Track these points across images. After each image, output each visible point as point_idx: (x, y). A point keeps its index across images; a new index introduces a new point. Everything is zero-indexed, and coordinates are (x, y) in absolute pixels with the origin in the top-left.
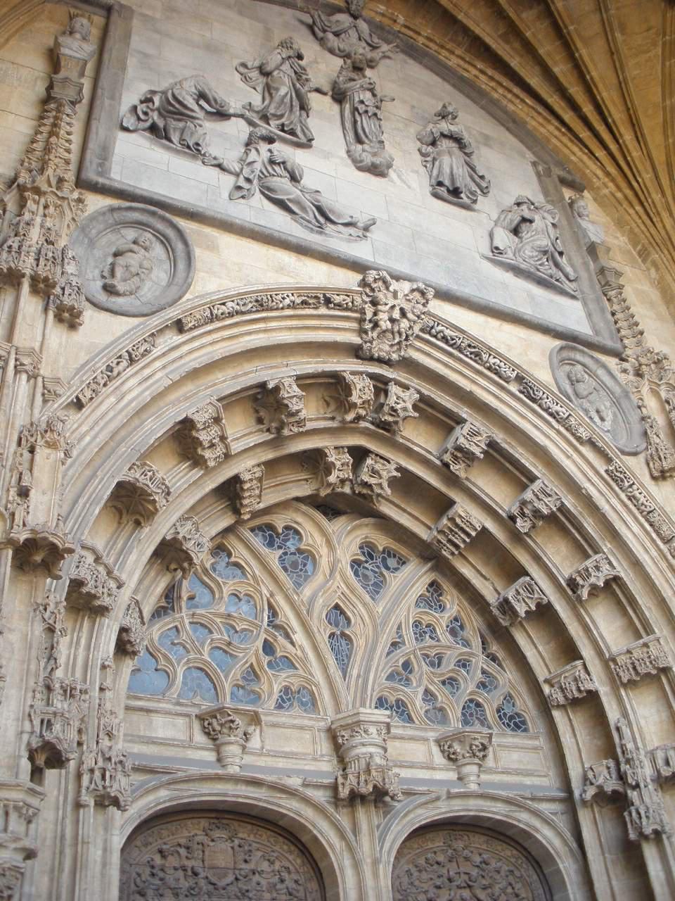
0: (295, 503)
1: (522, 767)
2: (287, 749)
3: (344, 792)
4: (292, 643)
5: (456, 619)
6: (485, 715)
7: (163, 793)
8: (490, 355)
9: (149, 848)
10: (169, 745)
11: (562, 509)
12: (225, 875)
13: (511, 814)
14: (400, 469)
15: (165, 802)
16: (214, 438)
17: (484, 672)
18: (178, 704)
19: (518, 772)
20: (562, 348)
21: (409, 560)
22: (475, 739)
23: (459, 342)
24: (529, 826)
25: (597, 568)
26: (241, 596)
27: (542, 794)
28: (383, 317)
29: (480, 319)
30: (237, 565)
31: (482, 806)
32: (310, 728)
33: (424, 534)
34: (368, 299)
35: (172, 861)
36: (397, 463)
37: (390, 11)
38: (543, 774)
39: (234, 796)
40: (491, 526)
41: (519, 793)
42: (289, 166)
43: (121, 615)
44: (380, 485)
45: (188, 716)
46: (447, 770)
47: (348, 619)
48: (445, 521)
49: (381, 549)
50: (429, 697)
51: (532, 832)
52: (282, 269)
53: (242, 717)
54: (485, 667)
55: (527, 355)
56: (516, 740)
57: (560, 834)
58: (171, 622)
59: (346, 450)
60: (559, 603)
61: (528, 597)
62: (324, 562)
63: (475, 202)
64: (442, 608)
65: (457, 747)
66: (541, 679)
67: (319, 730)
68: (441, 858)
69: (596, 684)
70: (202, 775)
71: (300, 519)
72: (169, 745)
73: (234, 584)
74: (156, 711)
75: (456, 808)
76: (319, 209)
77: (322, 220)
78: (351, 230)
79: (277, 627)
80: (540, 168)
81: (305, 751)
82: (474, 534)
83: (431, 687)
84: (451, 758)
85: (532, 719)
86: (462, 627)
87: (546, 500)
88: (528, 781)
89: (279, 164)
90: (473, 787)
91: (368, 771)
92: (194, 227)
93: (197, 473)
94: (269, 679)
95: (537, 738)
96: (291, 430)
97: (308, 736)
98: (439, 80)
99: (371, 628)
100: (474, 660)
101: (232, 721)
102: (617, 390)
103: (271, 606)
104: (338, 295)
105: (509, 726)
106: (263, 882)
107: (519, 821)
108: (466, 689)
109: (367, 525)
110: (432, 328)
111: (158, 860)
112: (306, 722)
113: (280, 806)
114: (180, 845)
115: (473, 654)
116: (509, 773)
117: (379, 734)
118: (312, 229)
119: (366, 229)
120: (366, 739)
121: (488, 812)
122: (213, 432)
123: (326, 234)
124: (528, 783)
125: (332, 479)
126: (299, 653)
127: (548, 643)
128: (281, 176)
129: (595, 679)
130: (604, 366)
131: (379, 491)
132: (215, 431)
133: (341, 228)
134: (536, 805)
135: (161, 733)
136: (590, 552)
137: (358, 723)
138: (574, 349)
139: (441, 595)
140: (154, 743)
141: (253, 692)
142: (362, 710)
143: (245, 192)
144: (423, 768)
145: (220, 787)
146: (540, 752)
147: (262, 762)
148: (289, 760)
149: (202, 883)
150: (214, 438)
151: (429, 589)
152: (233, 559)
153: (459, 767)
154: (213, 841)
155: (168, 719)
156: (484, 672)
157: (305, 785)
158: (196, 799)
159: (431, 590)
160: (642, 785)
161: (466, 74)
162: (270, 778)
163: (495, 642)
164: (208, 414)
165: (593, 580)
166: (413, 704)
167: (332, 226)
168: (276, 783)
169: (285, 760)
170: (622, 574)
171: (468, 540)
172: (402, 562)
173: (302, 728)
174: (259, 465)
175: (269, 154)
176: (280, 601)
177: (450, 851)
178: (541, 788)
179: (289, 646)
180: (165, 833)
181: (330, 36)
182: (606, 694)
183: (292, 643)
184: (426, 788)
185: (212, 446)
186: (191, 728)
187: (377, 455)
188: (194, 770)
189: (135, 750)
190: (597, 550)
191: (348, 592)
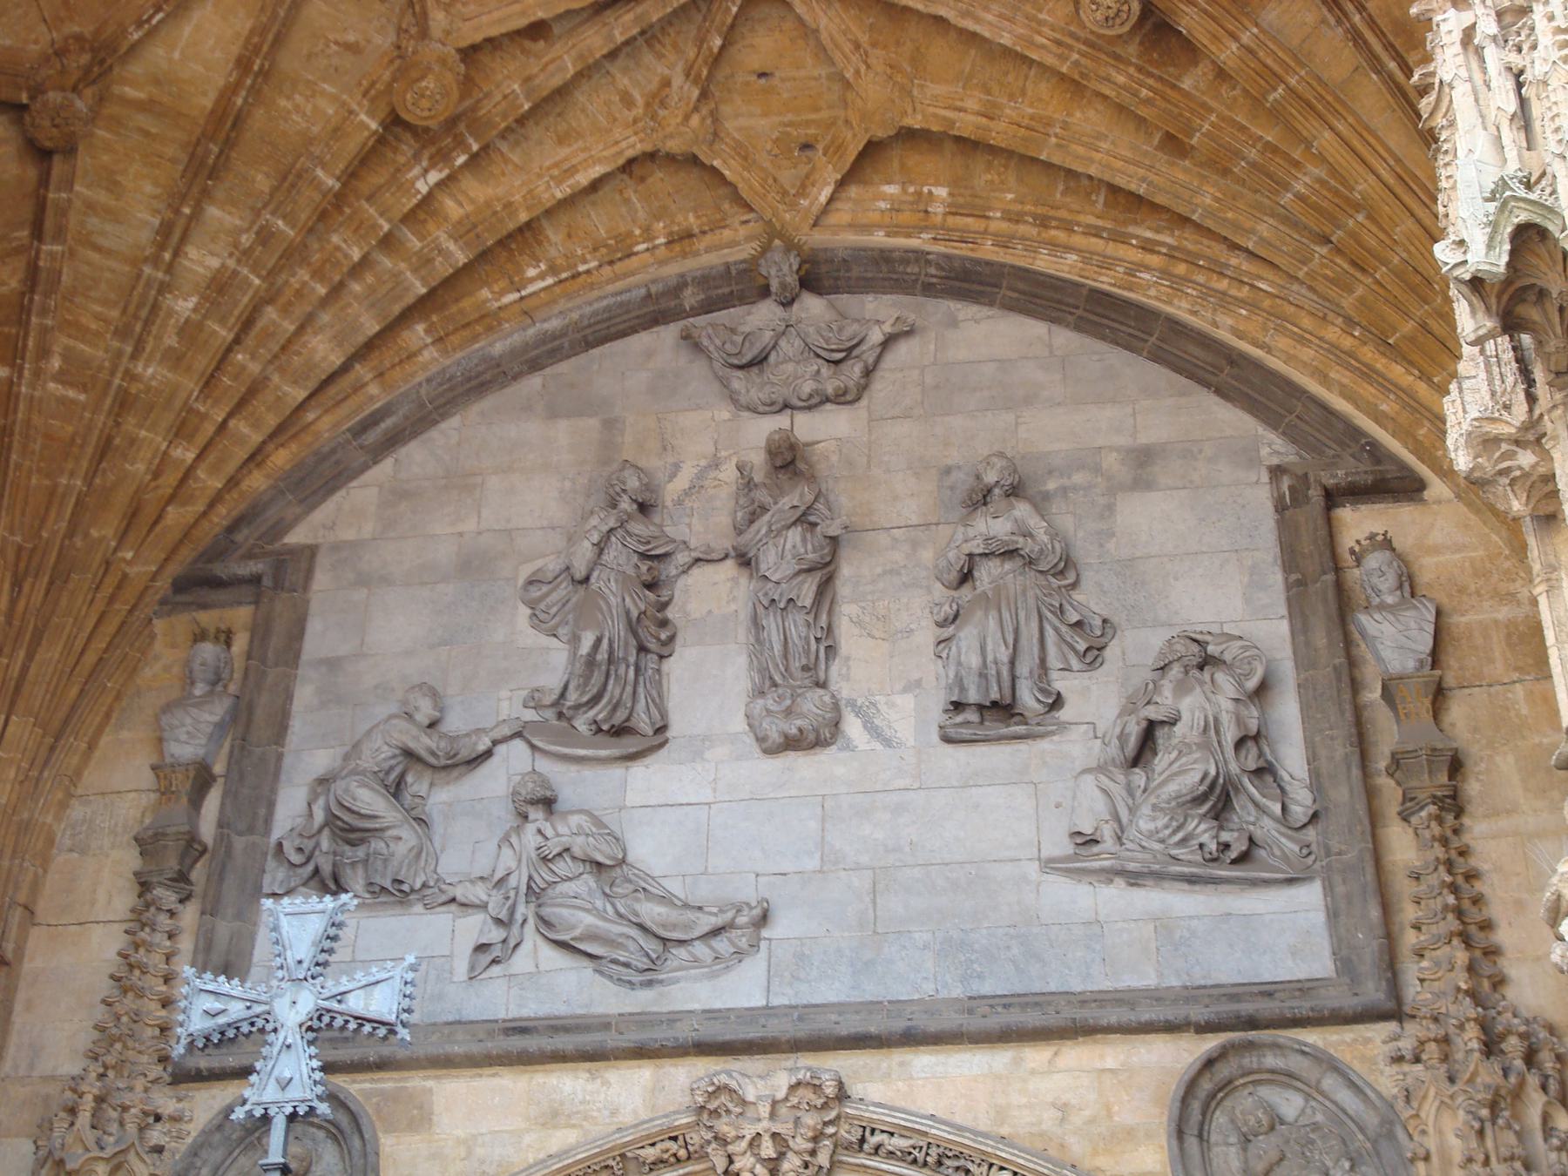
8: (991, 1165)
20: (1209, 1063)
23: (920, 1156)
29: (998, 1059)
34: (709, 1136)
37: (911, 190)
42: (577, 851)
52: (555, 1114)
55: (1110, 1115)
63: (1057, 702)
76: (642, 927)
77: (652, 946)
78: (722, 945)
80: (1286, 483)
89: (560, 854)
92: (389, 1085)
102: (1372, 1120)
104: (653, 1145)
110: (862, 1140)
118: (630, 982)
119: (764, 919)
123: (661, 982)
128: (570, 879)
130: (1334, 1067)
133: (700, 949)
138: (1250, 1046)
143: (496, 952)
161: (1105, 282)
167: (681, 952)
175: (540, 839)
181: (738, 381)
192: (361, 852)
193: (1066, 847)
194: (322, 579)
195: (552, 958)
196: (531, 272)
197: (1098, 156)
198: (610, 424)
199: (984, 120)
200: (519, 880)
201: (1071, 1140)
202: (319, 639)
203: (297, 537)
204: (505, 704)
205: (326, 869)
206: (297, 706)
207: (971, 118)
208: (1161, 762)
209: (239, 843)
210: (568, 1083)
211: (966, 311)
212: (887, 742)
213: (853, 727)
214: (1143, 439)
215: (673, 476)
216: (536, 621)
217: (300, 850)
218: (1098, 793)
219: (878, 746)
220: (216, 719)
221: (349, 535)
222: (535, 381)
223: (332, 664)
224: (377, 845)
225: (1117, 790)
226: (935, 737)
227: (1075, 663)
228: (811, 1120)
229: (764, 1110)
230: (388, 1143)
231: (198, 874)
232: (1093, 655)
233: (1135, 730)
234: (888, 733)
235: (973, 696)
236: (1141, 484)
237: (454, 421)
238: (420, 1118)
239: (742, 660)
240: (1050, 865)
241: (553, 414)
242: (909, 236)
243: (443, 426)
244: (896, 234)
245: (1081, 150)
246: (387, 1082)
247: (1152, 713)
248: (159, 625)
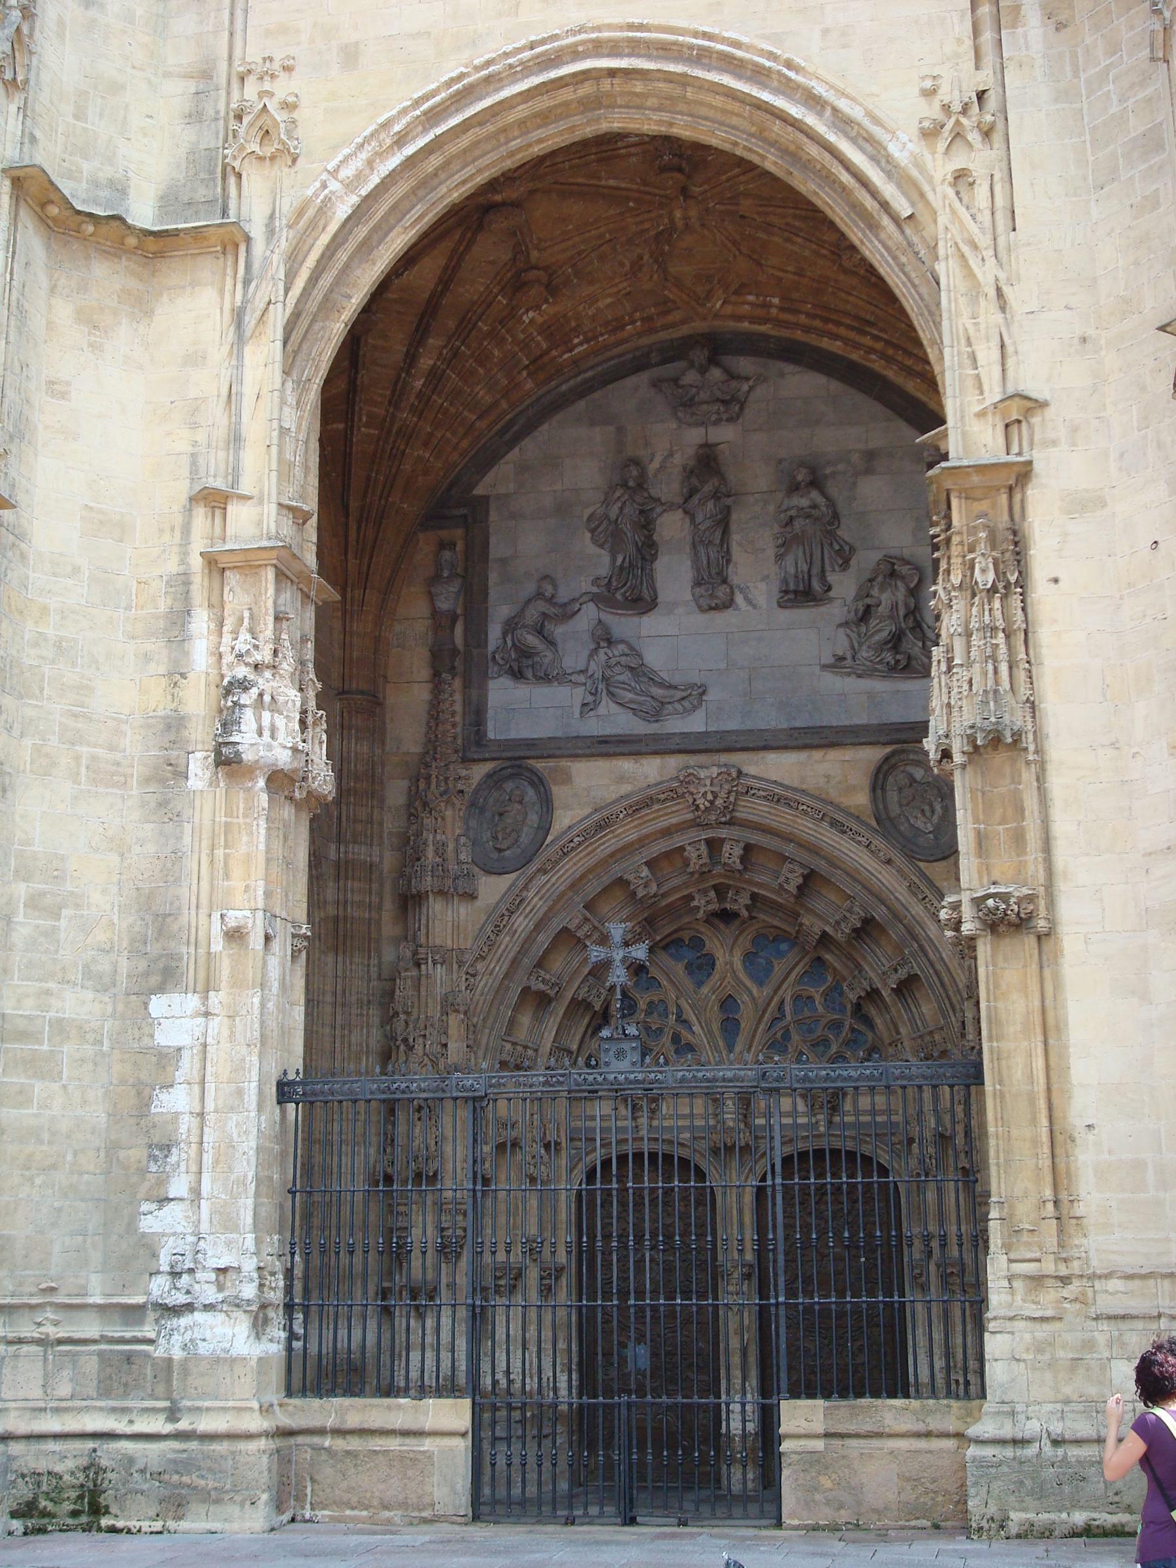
20: (887, 759)
25: (896, 970)
28: (700, 802)
63: (829, 588)
78: (686, 703)
98: (822, 379)
132: (586, 928)
156: (853, 1030)
167: (669, 707)
179: (690, 1037)
192: (530, 662)
193: (831, 660)
194: (493, 516)
195: (614, 708)
196: (576, 341)
197: (851, 299)
198: (620, 430)
199: (796, 278)
200: (598, 675)
201: (831, 791)
202: (497, 548)
203: (479, 491)
204: (583, 584)
205: (516, 668)
206: (491, 583)
207: (791, 276)
208: (873, 622)
209: (475, 652)
210: (626, 765)
211: (789, 368)
212: (755, 607)
213: (739, 599)
214: (872, 445)
215: (652, 460)
216: (594, 541)
217: (503, 659)
218: (846, 639)
219: (749, 608)
220: (455, 590)
221: (502, 490)
222: (581, 404)
223: (503, 561)
224: (537, 659)
225: (854, 636)
226: (775, 605)
227: (837, 568)
228: (727, 787)
229: (708, 782)
230: (555, 790)
231: (458, 663)
232: (845, 565)
233: (861, 609)
234: (754, 602)
235: (792, 587)
236: (869, 471)
237: (545, 426)
238: (567, 779)
239: (689, 563)
240: (825, 667)
241: (593, 423)
242: (760, 324)
243: (540, 429)
244: (754, 323)
245: (843, 295)
246: (551, 763)
247: (868, 601)
248: (421, 536)
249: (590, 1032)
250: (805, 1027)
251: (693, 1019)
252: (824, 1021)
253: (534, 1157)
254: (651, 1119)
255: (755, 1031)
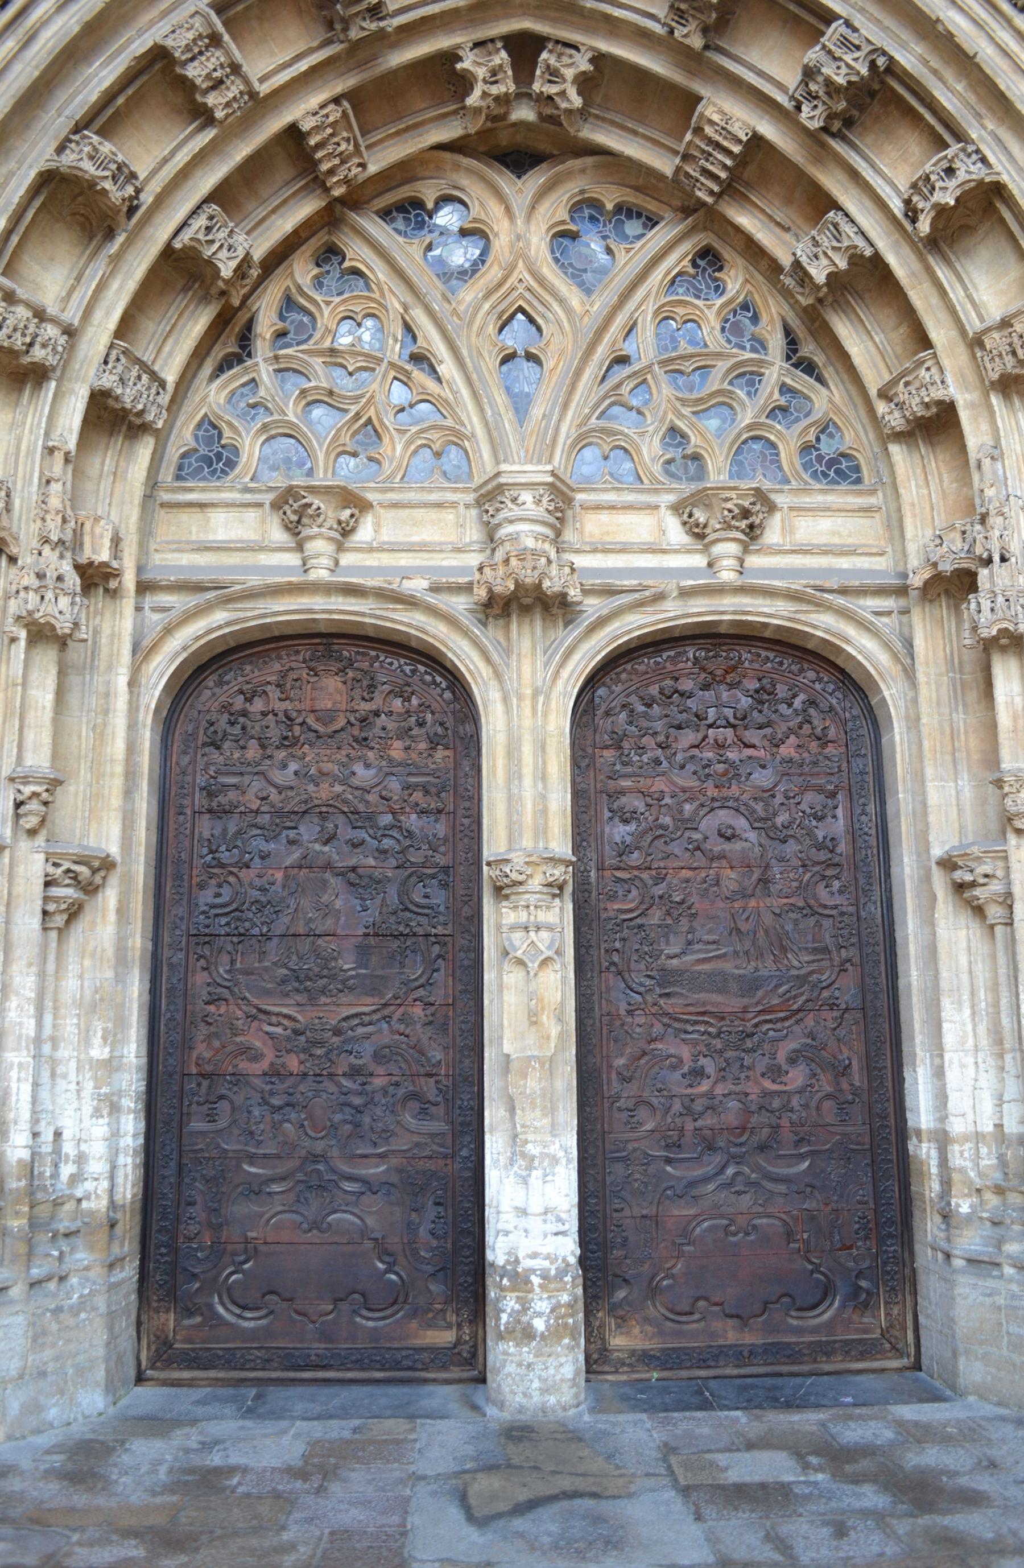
0: (447, 155)
1: (836, 540)
2: (416, 539)
3: (482, 593)
4: (439, 380)
5: (745, 307)
6: (778, 461)
7: (220, 616)
9: (225, 688)
10: (230, 549)
11: (893, 68)
12: (332, 720)
13: (798, 616)
14: (599, 59)
15: (220, 627)
16: (215, 70)
17: (785, 389)
18: (246, 490)
19: (826, 551)
21: (662, 218)
22: (727, 500)
24: (833, 635)
25: (950, 171)
26: (359, 318)
27: (857, 583)
30: (356, 272)
31: (747, 605)
32: (454, 505)
33: (665, 165)
35: (258, 705)
36: (592, 49)
38: (874, 550)
39: (324, 611)
40: (768, 130)
41: (812, 582)
43: (92, 372)
44: (563, 94)
45: (259, 505)
46: (689, 551)
47: (539, 329)
48: (688, 137)
49: (610, 206)
50: (679, 439)
51: (838, 642)
53: (326, 498)
54: (789, 381)
56: (831, 499)
57: (887, 646)
58: (243, 375)
59: (499, 45)
60: (897, 253)
61: (834, 248)
62: (501, 243)
64: (719, 289)
65: (700, 516)
66: (873, 392)
67: (467, 506)
68: (687, 685)
69: (951, 389)
70: (268, 586)
71: (464, 181)
72: (230, 549)
73: (344, 301)
74: (213, 505)
75: (695, 610)
79: (417, 358)
81: (443, 539)
82: (736, 149)
83: (679, 423)
84: (698, 533)
85: (868, 463)
86: (755, 319)
87: (848, 58)
88: (844, 563)
90: (727, 576)
91: (507, 561)
93: (209, 134)
94: (392, 438)
95: (873, 492)
96: (363, 29)
97: (451, 517)
99: (570, 336)
100: (767, 372)
101: (309, 505)
103: (408, 328)
105: (825, 475)
106: (391, 726)
107: (815, 627)
108: (741, 421)
109: (583, 171)
111: (239, 702)
112: (450, 496)
113: (393, 621)
114: (269, 683)
115: (762, 361)
116: (806, 552)
117: (538, 502)
120: (517, 512)
121: (758, 614)
122: (213, 60)
124: (845, 566)
125: (473, 99)
126: (447, 394)
127: (897, 327)
129: (949, 380)
131: (564, 105)
134: (840, 601)
135: (221, 534)
136: (947, 137)
137: (500, 488)
139: (720, 269)
140: (208, 549)
141: (371, 459)
142: (504, 467)
144: (644, 551)
145: (304, 601)
146: (877, 515)
147: (372, 560)
148: (419, 555)
149: (297, 730)
150: (215, 70)
151: (700, 262)
152: (347, 264)
153: (707, 548)
154: (316, 675)
155: (234, 514)
156: (785, 389)
157: (435, 589)
158: (268, 620)
159: (702, 263)
160: (996, 558)
162: (370, 582)
163: (810, 338)
164: (192, 32)
165: (938, 197)
166: (639, 452)
168: (380, 588)
169: (410, 555)
170: (1005, 178)
171: (729, 162)
172: (651, 222)
173: (439, 505)
174: (336, 100)
176: (419, 317)
177: (703, 675)
178: (872, 573)
179: (431, 385)
180: (248, 668)
182: (972, 406)
183: (439, 380)
184: (635, 582)
185: (218, 84)
186: (263, 521)
187: (557, 42)
188: (254, 581)
189: (184, 562)
190: (960, 136)
191: (533, 283)
249: (208, 369)
250: (681, 380)
251: (440, 349)
252: (722, 366)
253: (40, 576)
254: (340, 548)
255: (578, 373)
